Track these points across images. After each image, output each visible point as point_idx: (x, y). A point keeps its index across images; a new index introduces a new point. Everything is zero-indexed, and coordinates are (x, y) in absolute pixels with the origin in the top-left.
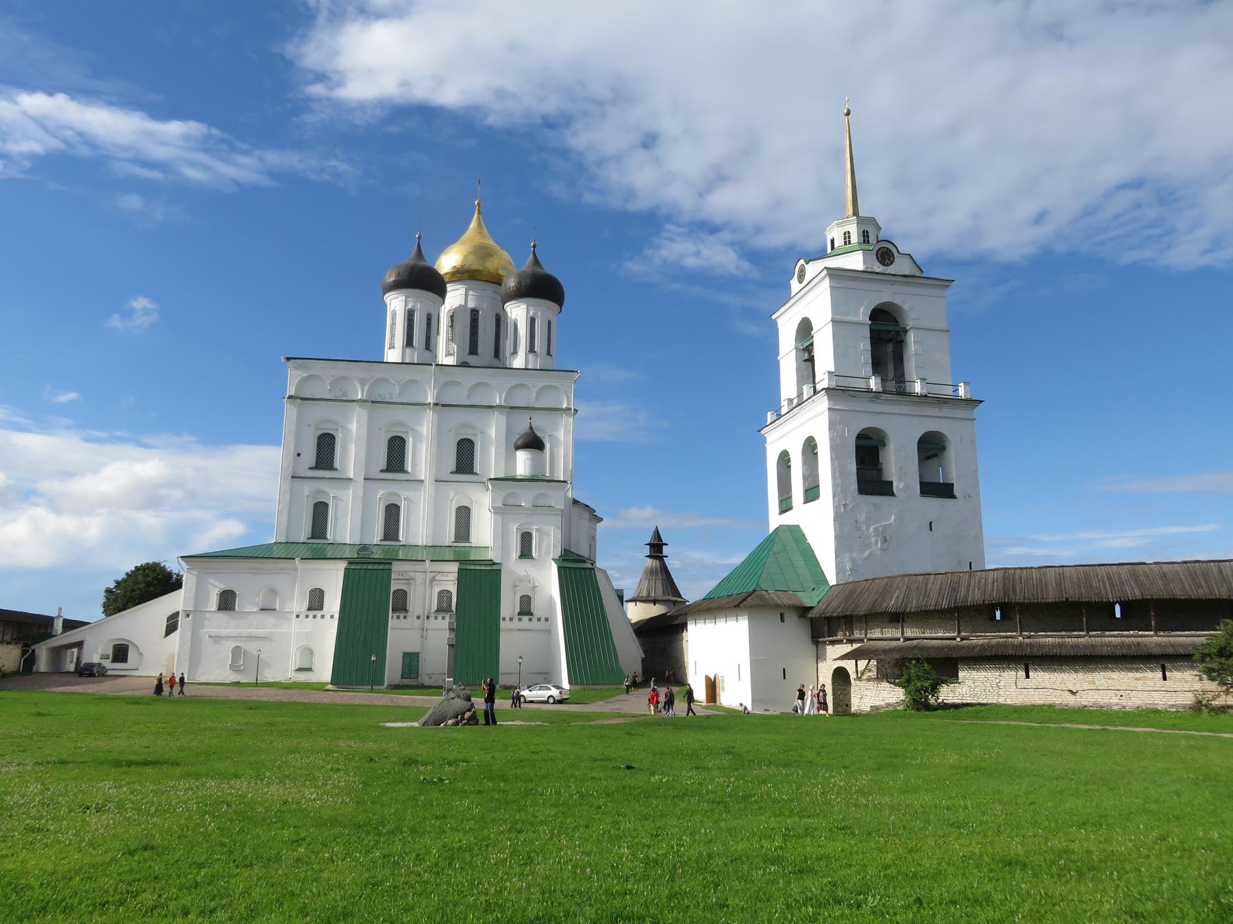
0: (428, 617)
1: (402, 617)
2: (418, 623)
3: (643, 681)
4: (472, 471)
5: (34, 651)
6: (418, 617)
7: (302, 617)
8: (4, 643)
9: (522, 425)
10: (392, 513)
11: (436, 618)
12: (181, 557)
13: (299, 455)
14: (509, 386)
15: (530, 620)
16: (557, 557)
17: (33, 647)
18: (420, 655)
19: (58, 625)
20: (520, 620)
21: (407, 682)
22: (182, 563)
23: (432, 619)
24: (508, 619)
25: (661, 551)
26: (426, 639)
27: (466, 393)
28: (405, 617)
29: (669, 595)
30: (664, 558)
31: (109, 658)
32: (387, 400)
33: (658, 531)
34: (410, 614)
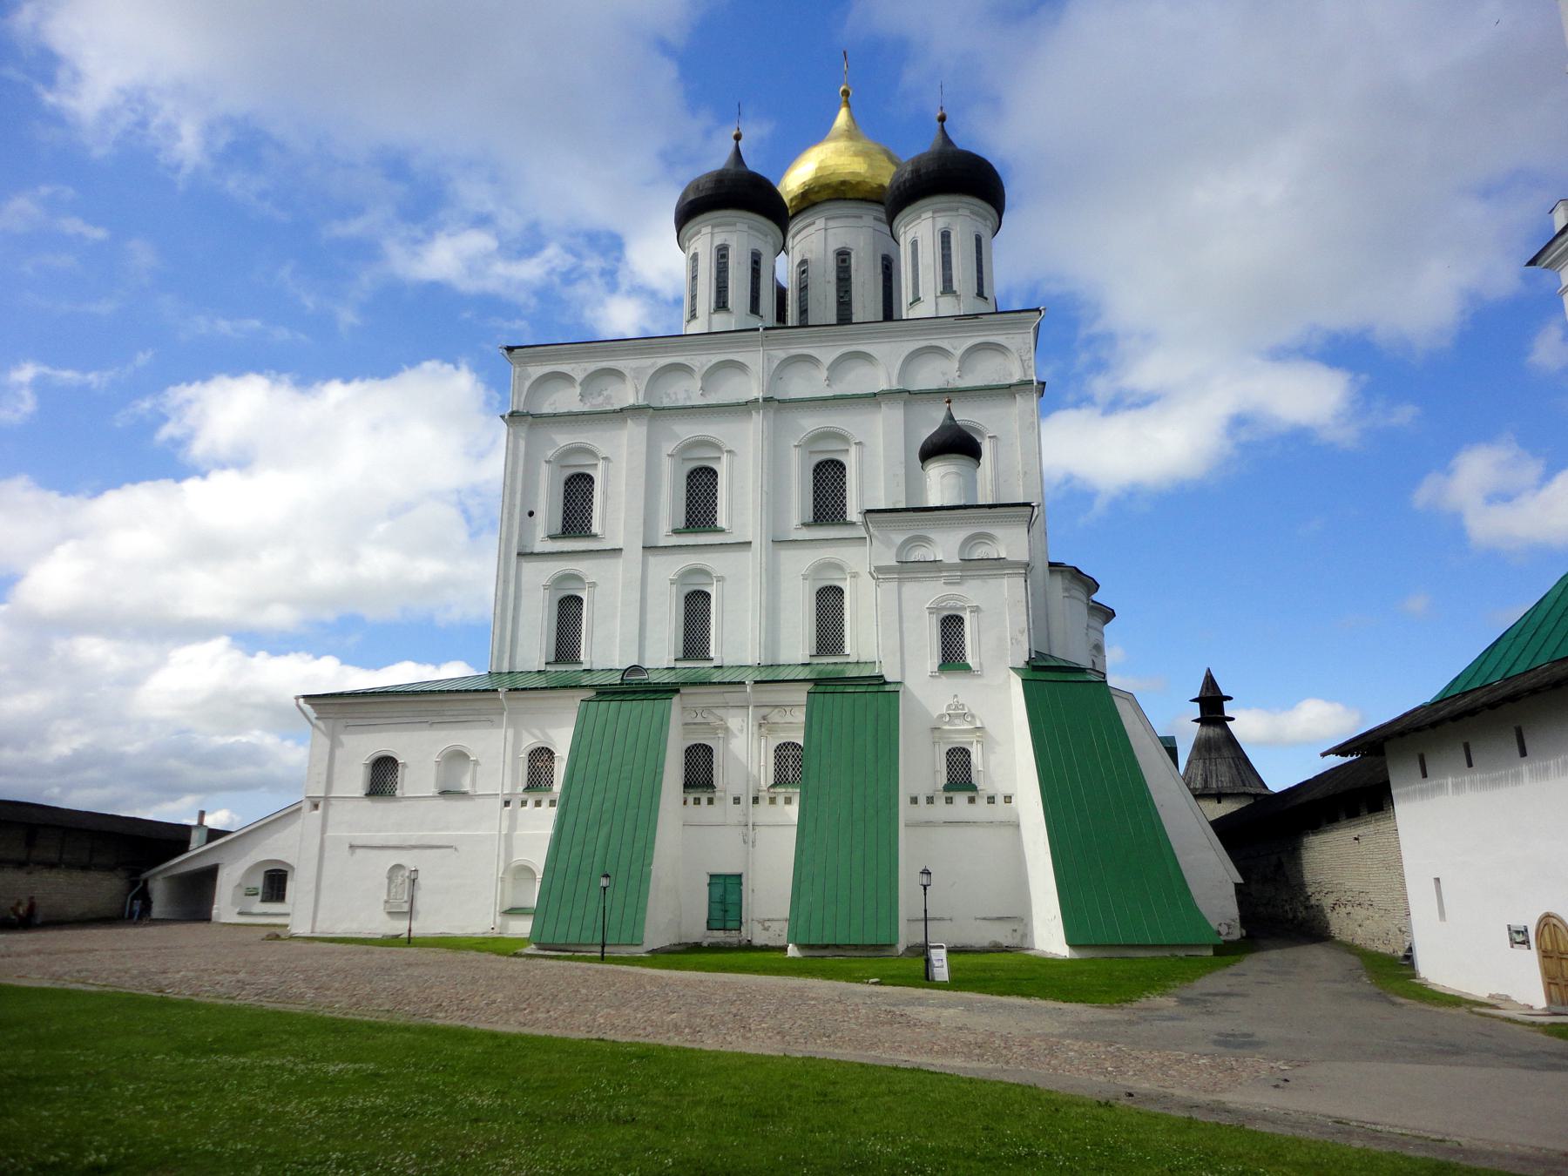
0: (756, 800)
1: (704, 801)
2: (735, 813)
3: (1242, 937)
4: (845, 519)
5: (146, 882)
6: (737, 800)
7: (516, 803)
8: (90, 869)
9: (931, 422)
10: (696, 606)
11: (773, 801)
12: (304, 697)
13: (531, 514)
14: (906, 353)
15: (972, 800)
16: (1021, 664)
17: (144, 876)
18: (744, 880)
19: (196, 838)
20: (949, 801)
21: (719, 936)
22: (307, 707)
23: (764, 803)
24: (922, 800)
25: (1222, 711)
26: (753, 846)
27: (825, 374)
28: (710, 801)
29: (1245, 785)
30: (1228, 723)
31: (257, 894)
32: (680, 404)
33: (1211, 676)
34: (717, 794)
